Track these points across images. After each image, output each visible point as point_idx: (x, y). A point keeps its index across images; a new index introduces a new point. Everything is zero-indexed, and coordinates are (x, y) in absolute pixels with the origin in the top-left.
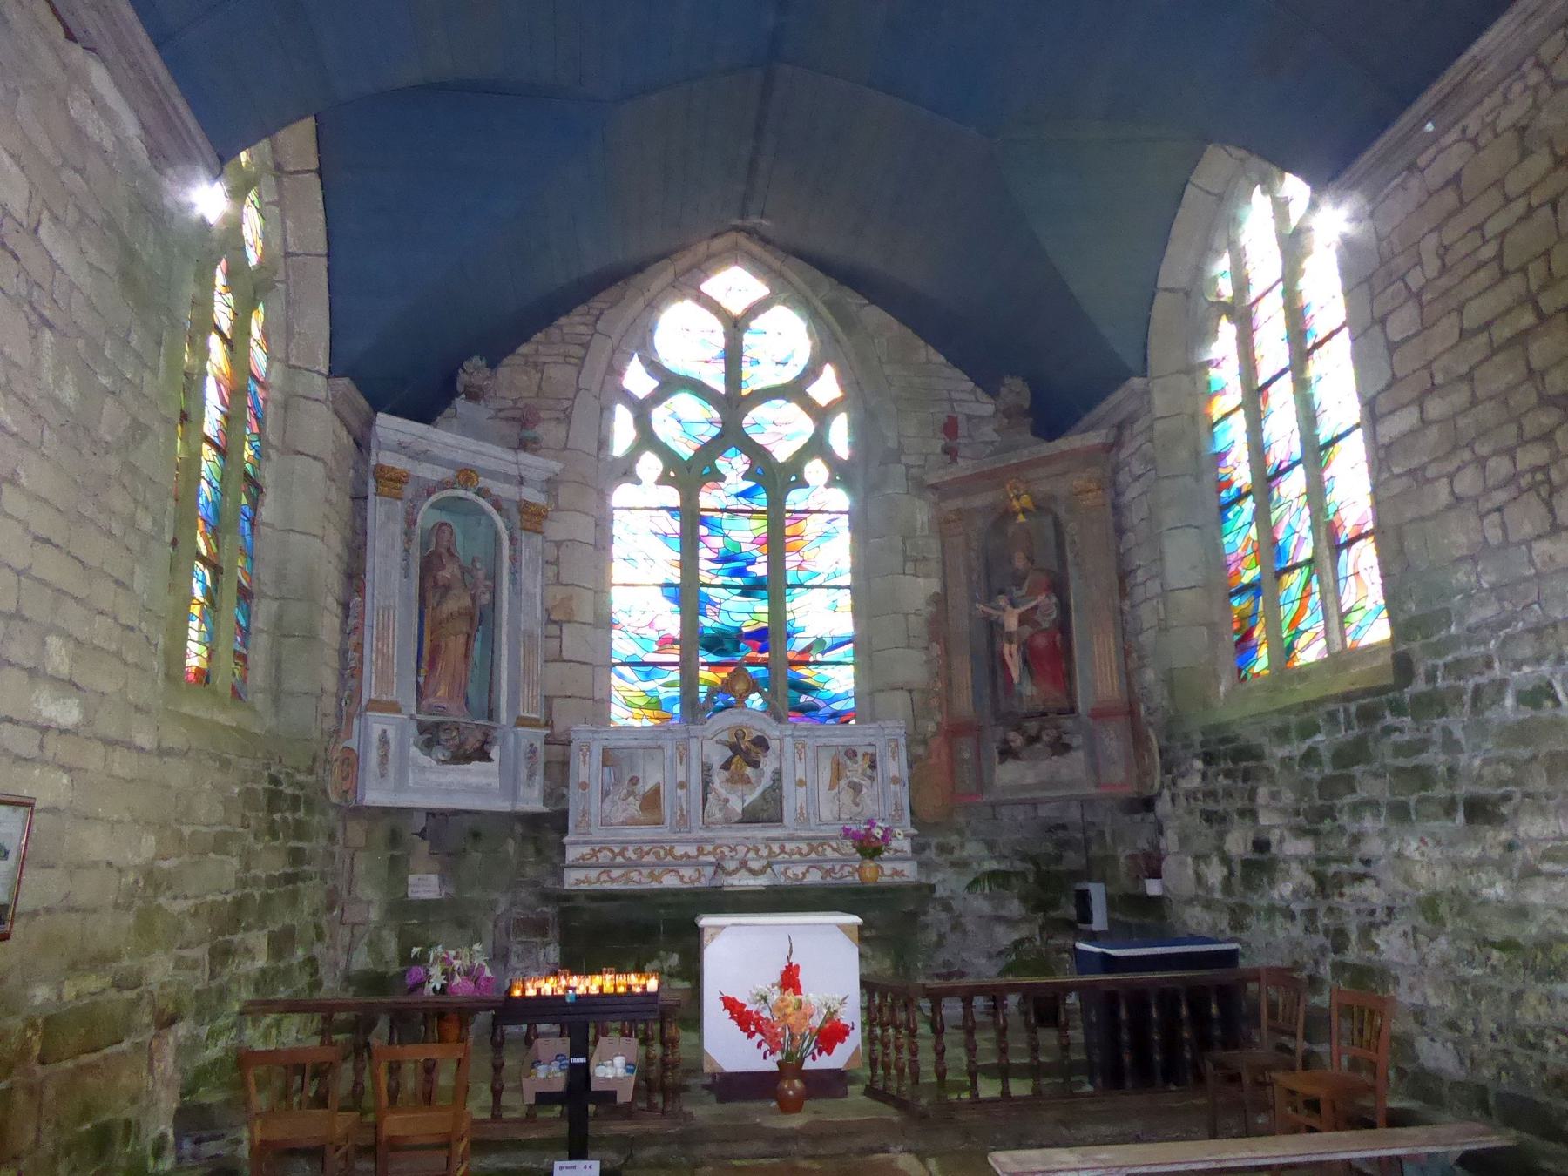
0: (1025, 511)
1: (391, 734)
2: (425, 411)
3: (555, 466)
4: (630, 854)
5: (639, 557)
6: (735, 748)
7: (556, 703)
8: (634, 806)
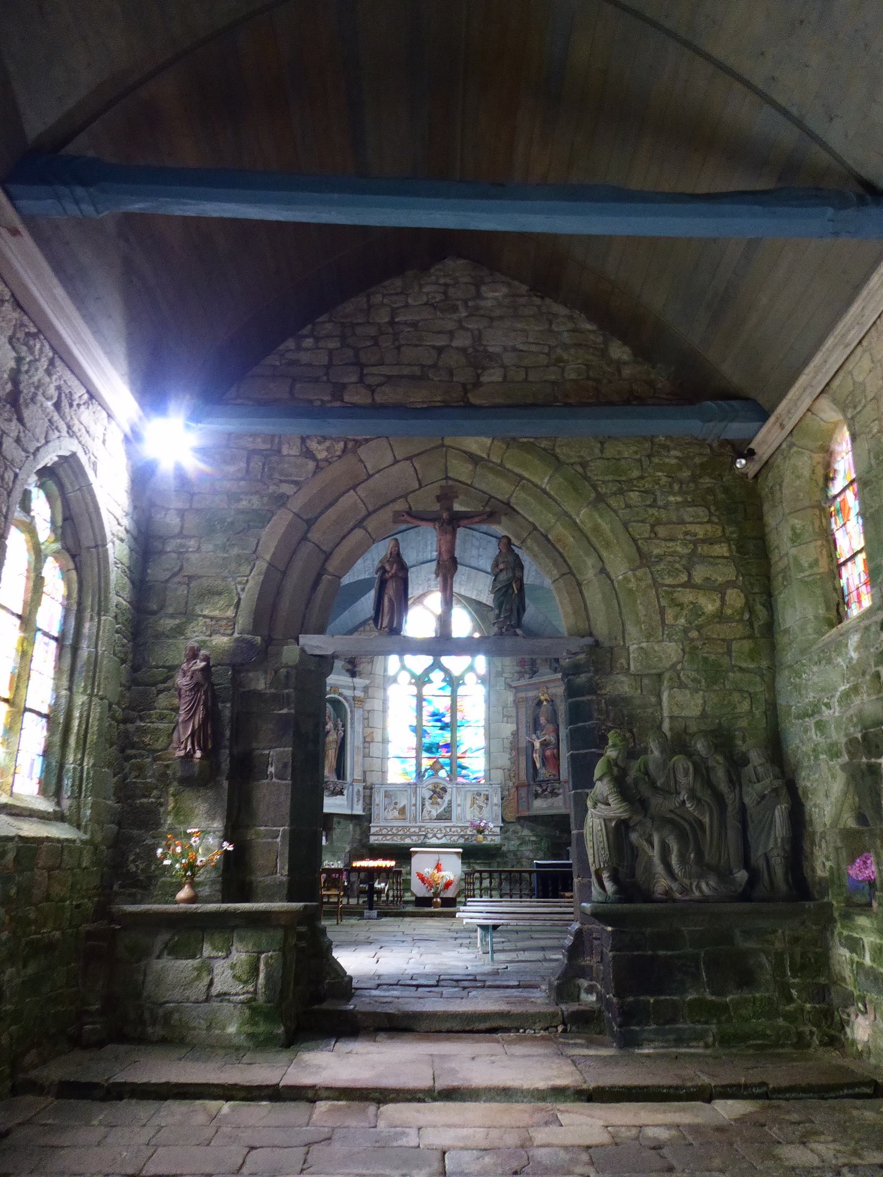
0: (546, 700)
3: (367, 682)
6: (434, 792)
8: (396, 813)
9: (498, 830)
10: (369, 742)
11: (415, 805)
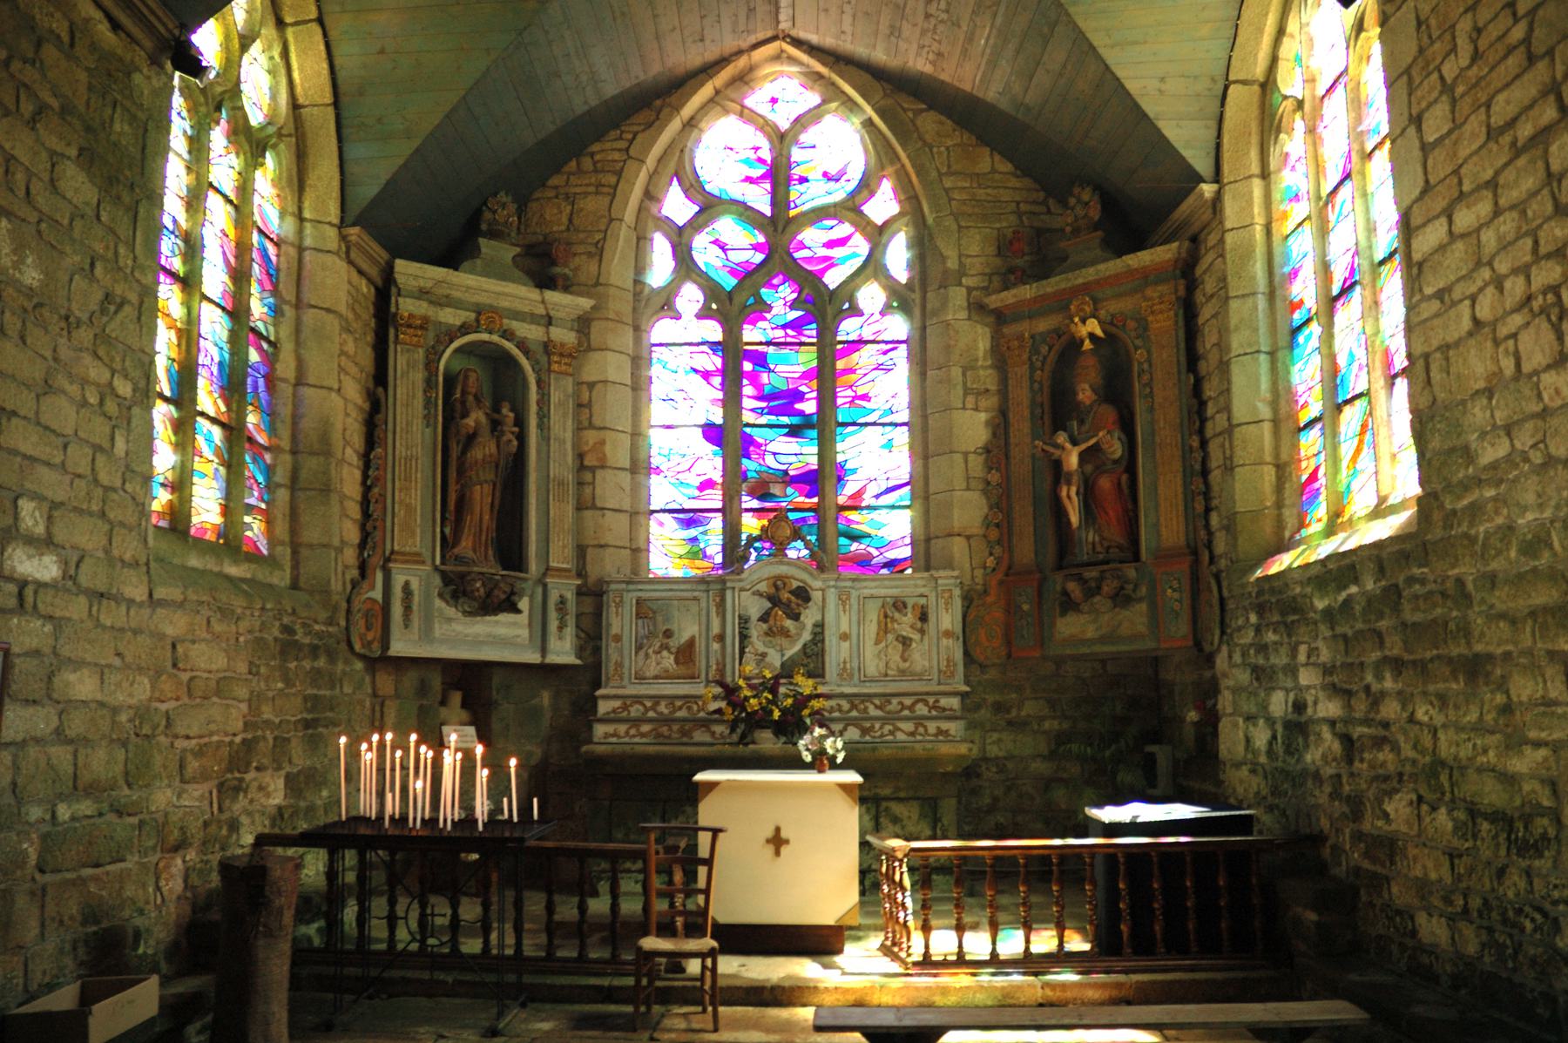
1: (415, 585)
2: (453, 255)
3: (585, 303)
4: (663, 708)
5: (679, 396)
6: (774, 600)
7: (590, 553)
8: (668, 661)
9: (954, 702)
10: (593, 469)
11: (721, 638)
